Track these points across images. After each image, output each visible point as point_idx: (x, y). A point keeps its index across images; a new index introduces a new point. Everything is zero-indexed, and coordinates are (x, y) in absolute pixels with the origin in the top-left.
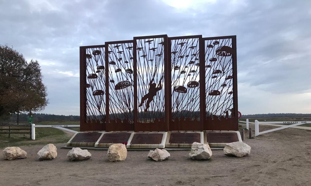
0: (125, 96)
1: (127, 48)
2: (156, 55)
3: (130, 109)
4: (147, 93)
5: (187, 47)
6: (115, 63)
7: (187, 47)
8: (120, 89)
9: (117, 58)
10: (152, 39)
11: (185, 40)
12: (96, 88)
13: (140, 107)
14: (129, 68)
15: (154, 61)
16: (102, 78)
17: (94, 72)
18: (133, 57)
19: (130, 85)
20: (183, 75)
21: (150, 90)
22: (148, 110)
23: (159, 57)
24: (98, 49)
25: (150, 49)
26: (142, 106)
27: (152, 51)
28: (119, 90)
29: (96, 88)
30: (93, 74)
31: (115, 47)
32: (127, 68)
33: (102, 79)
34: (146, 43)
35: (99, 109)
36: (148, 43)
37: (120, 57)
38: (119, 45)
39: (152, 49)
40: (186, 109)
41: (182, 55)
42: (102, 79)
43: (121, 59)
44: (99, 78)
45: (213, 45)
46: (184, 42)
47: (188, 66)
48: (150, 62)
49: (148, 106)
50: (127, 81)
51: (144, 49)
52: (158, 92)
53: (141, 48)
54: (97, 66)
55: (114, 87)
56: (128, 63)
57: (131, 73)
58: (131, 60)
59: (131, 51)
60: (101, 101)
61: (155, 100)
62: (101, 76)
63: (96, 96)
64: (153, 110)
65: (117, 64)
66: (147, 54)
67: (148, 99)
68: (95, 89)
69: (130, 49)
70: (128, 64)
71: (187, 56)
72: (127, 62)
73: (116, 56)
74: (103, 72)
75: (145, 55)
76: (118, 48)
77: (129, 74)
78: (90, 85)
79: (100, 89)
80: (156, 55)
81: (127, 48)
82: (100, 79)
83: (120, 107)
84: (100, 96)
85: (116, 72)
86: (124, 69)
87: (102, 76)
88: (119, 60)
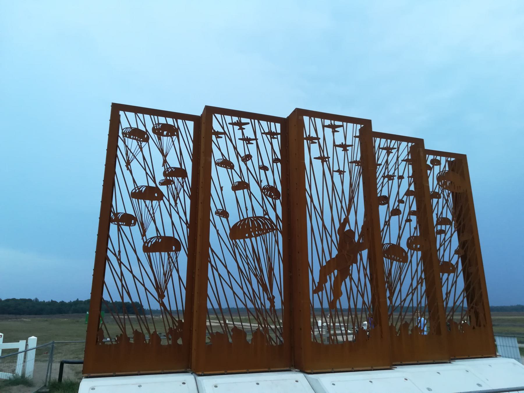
0: (259, 260)
1: (265, 133)
2: (350, 161)
3: (272, 300)
4: (334, 256)
5: (398, 158)
6: (233, 166)
7: (398, 158)
8: (244, 238)
9: (237, 154)
10: (340, 123)
11: (393, 142)
12: (157, 230)
13: (316, 295)
14: (271, 184)
15: (347, 175)
16: (178, 201)
17: (155, 181)
18: (280, 157)
19: (273, 230)
20: (394, 220)
21: (340, 248)
22: (338, 306)
23: (357, 167)
24: (170, 121)
25: (335, 145)
26: (322, 291)
27: (340, 150)
28: (242, 241)
29: (157, 230)
30: (148, 188)
31: (233, 124)
32: (264, 184)
33: (176, 204)
34: (325, 128)
35: (161, 296)
36: (331, 130)
37: (247, 153)
38: (244, 120)
39: (339, 146)
40: (411, 305)
41: (391, 173)
42: (176, 204)
43: (248, 157)
44: (169, 201)
45: (431, 166)
46: (391, 147)
47: (404, 199)
48: (336, 175)
49: (337, 292)
50: (266, 219)
51: (321, 141)
52: (361, 255)
53: (315, 139)
54: (163, 165)
55: (228, 232)
56: (268, 170)
57: (276, 199)
58: (275, 164)
59: (275, 141)
60: (171, 270)
61: (355, 276)
62: (176, 198)
63: (155, 256)
64: (352, 306)
65: (237, 168)
66: (330, 155)
67: (336, 271)
68: (151, 233)
69: (274, 138)
70: (269, 173)
71: (401, 177)
72: (265, 168)
73: (235, 148)
74: (183, 187)
75: (326, 156)
76: (242, 129)
77: (270, 199)
78: (135, 219)
79: (169, 234)
80: (351, 162)
81: (265, 133)
82: (170, 204)
83: (244, 293)
84: (169, 255)
85: (236, 188)
86: (258, 183)
87: (178, 197)
88: (243, 160)
